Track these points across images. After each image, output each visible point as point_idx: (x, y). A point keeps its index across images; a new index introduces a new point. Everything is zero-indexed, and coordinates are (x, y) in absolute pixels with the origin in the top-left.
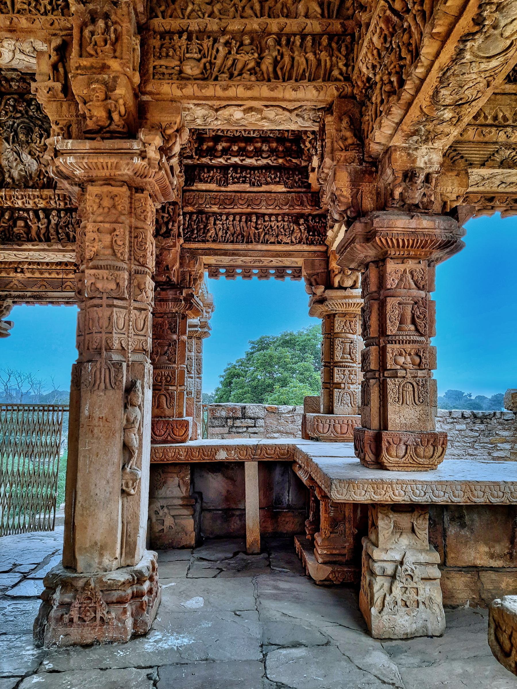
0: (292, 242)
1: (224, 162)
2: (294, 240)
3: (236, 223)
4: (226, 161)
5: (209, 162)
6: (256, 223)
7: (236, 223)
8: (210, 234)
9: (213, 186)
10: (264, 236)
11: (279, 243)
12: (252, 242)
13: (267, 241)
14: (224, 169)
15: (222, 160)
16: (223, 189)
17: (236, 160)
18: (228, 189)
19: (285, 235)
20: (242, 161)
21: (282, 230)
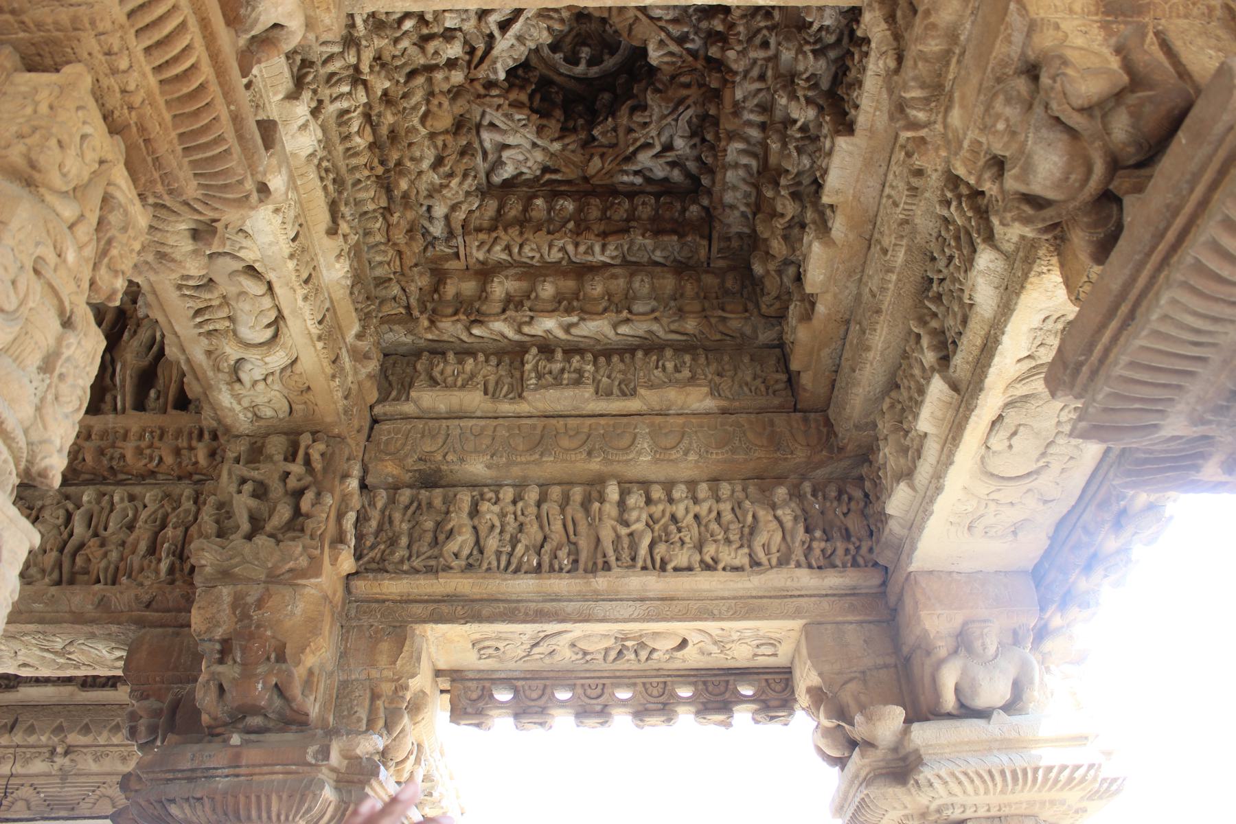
0: (755, 563)
1: (510, 333)
2: (761, 555)
3: (551, 508)
4: (519, 331)
5: (464, 337)
6: (621, 504)
7: (551, 508)
8: (453, 546)
9: (473, 399)
10: (652, 546)
11: (709, 567)
12: (607, 567)
13: (664, 565)
14: (512, 354)
15: (501, 327)
16: (506, 407)
17: (548, 325)
18: (523, 408)
19: (728, 541)
20: (567, 328)
21: (714, 526)
